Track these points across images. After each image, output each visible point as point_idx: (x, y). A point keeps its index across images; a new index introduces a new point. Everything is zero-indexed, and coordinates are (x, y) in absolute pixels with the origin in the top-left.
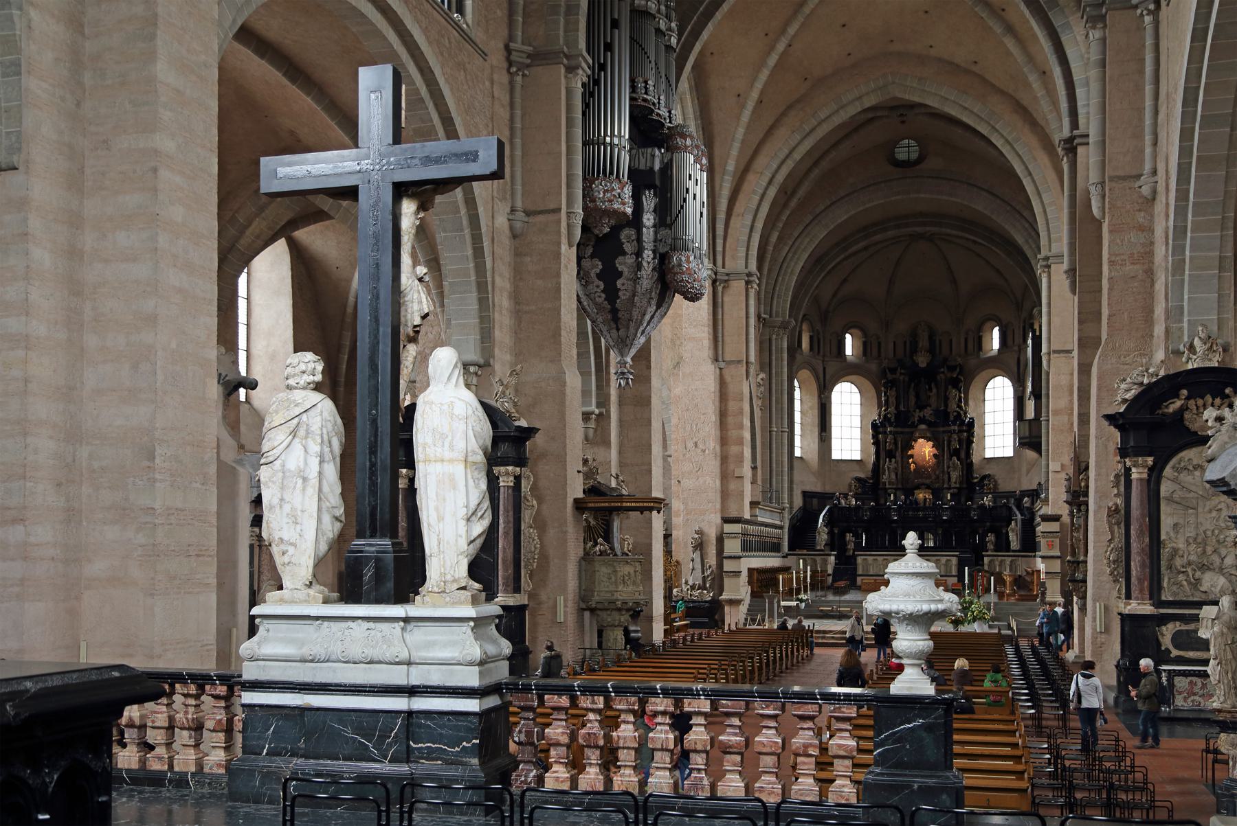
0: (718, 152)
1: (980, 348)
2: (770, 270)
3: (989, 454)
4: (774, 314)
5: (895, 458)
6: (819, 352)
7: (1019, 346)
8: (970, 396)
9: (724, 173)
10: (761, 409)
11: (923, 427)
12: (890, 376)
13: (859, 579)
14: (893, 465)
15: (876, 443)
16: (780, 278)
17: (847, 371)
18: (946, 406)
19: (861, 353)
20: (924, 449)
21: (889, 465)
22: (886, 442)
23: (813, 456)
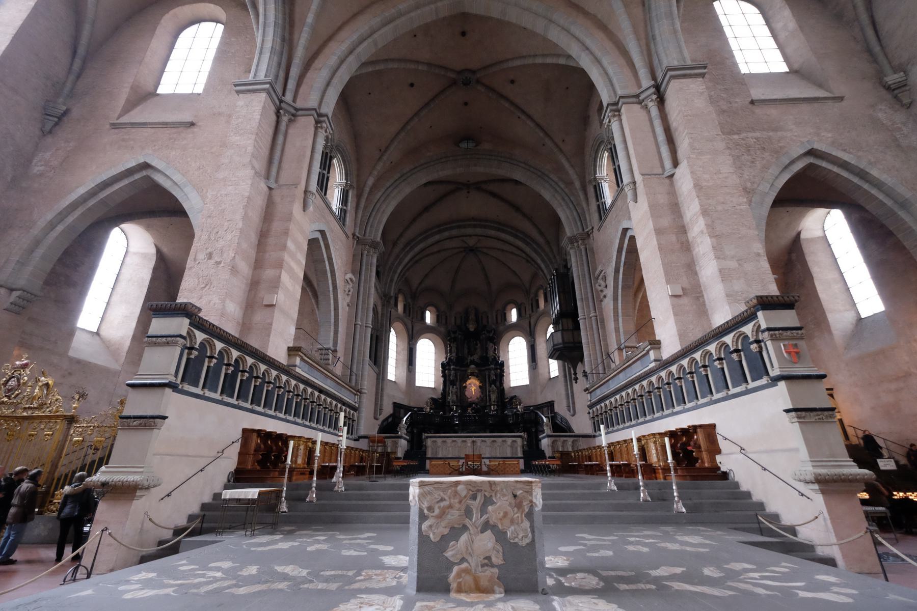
0: (298, 10)
1: (505, 320)
2: (365, 208)
3: (513, 384)
4: (367, 234)
5: (456, 385)
6: (409, 316)
7: (530, 315)
8: (501, 348)
9: (304, 24)
10: (348, 305)
11: (473, 366)
12: (453, 336)
13: (428, 462)
14: (455, 390)
15: (444, 376)
16: (374, 213)
17: (426, 331)
18: (487, 353)
19: (436, 321)
20: (473, 386)
21: (452, 389)
22: (450, 375)
23: (402, 381)
